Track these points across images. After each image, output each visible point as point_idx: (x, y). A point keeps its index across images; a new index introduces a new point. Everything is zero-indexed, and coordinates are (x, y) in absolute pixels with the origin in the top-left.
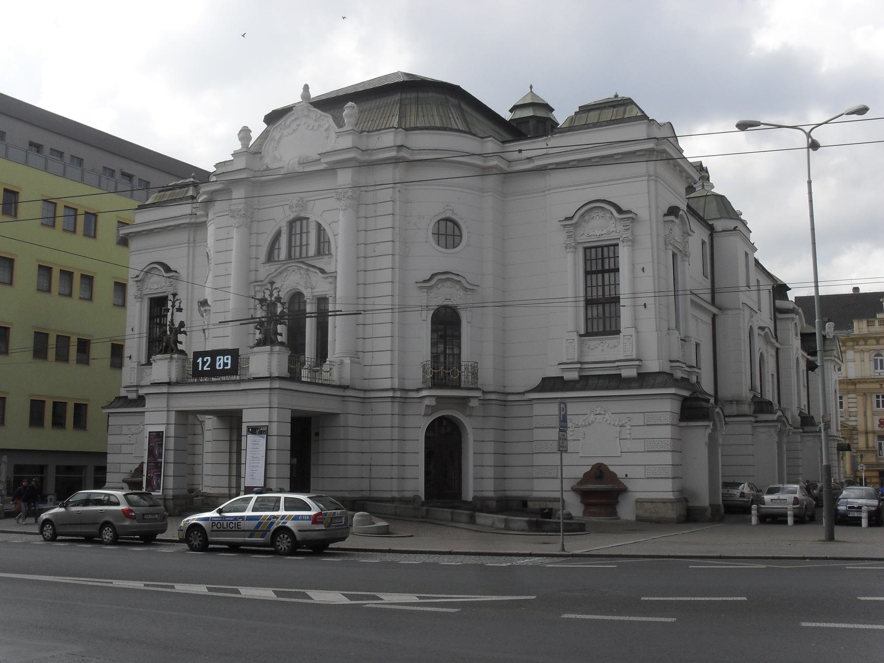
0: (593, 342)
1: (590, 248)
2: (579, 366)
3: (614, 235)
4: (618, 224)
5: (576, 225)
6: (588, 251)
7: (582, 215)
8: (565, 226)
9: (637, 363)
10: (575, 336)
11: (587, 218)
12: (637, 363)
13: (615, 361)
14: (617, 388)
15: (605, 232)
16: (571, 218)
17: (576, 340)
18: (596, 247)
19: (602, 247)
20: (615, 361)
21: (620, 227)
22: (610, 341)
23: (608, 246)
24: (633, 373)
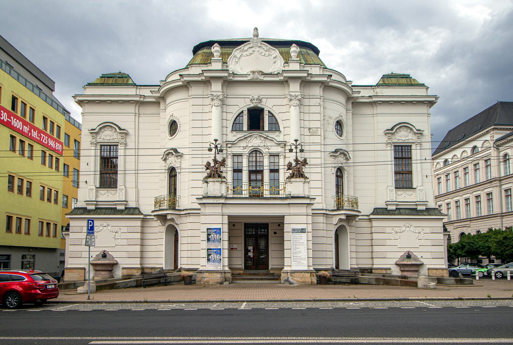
0: (102, 191)
1: (104, 145)
2: (95, 203)
3: (116, 140)
4: (119, 135)
5: (97, 133)
6: (103, 147)
7: (101, 129)
8: (91, 133)
9: (125, 203)
10: (94, 187)
11: (103, 130)
12: (125, 203)
13: (114, 202)
14: (115, 214)
15: (112, 138)
16: (94, 130)
17: (94, 191)
18: (107, 145)
19: (110, 146)
20: (114, 202)
21: (119, 136)
22: (112, 191)
23: (113, 145)
24: (123, 207)
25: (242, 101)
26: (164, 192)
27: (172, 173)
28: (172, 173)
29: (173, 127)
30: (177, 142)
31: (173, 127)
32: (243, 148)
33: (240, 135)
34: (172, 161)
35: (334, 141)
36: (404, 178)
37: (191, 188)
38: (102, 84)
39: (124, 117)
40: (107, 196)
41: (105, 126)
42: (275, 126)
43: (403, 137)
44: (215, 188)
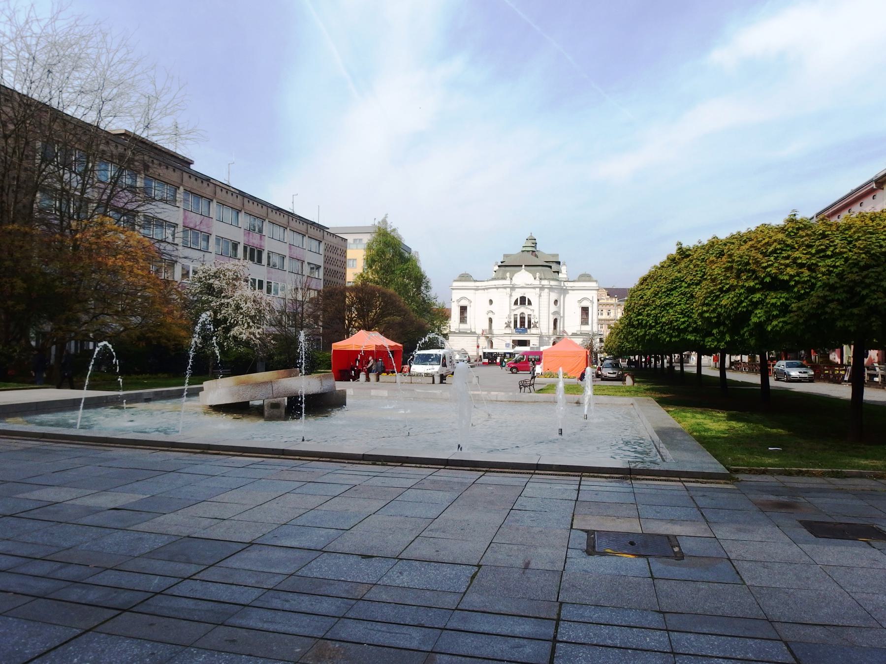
25: (517, 295)
26: (486, 327)
27: (491, 320)
28: (491, 320)
29: (491, 302)
30: (491, 308)
31: (491, 302)
32: (518, 312)
33: (516, 307)
34: (491, 315)
35: (553, 308)
36: (585, 321)
37: (499, 327)
38: (460, 281)
39: (469, 294)
40: (463, 327)
41: (462, 298)
42: (530, 303)
43: (585, 304)
44: (508, 331)
